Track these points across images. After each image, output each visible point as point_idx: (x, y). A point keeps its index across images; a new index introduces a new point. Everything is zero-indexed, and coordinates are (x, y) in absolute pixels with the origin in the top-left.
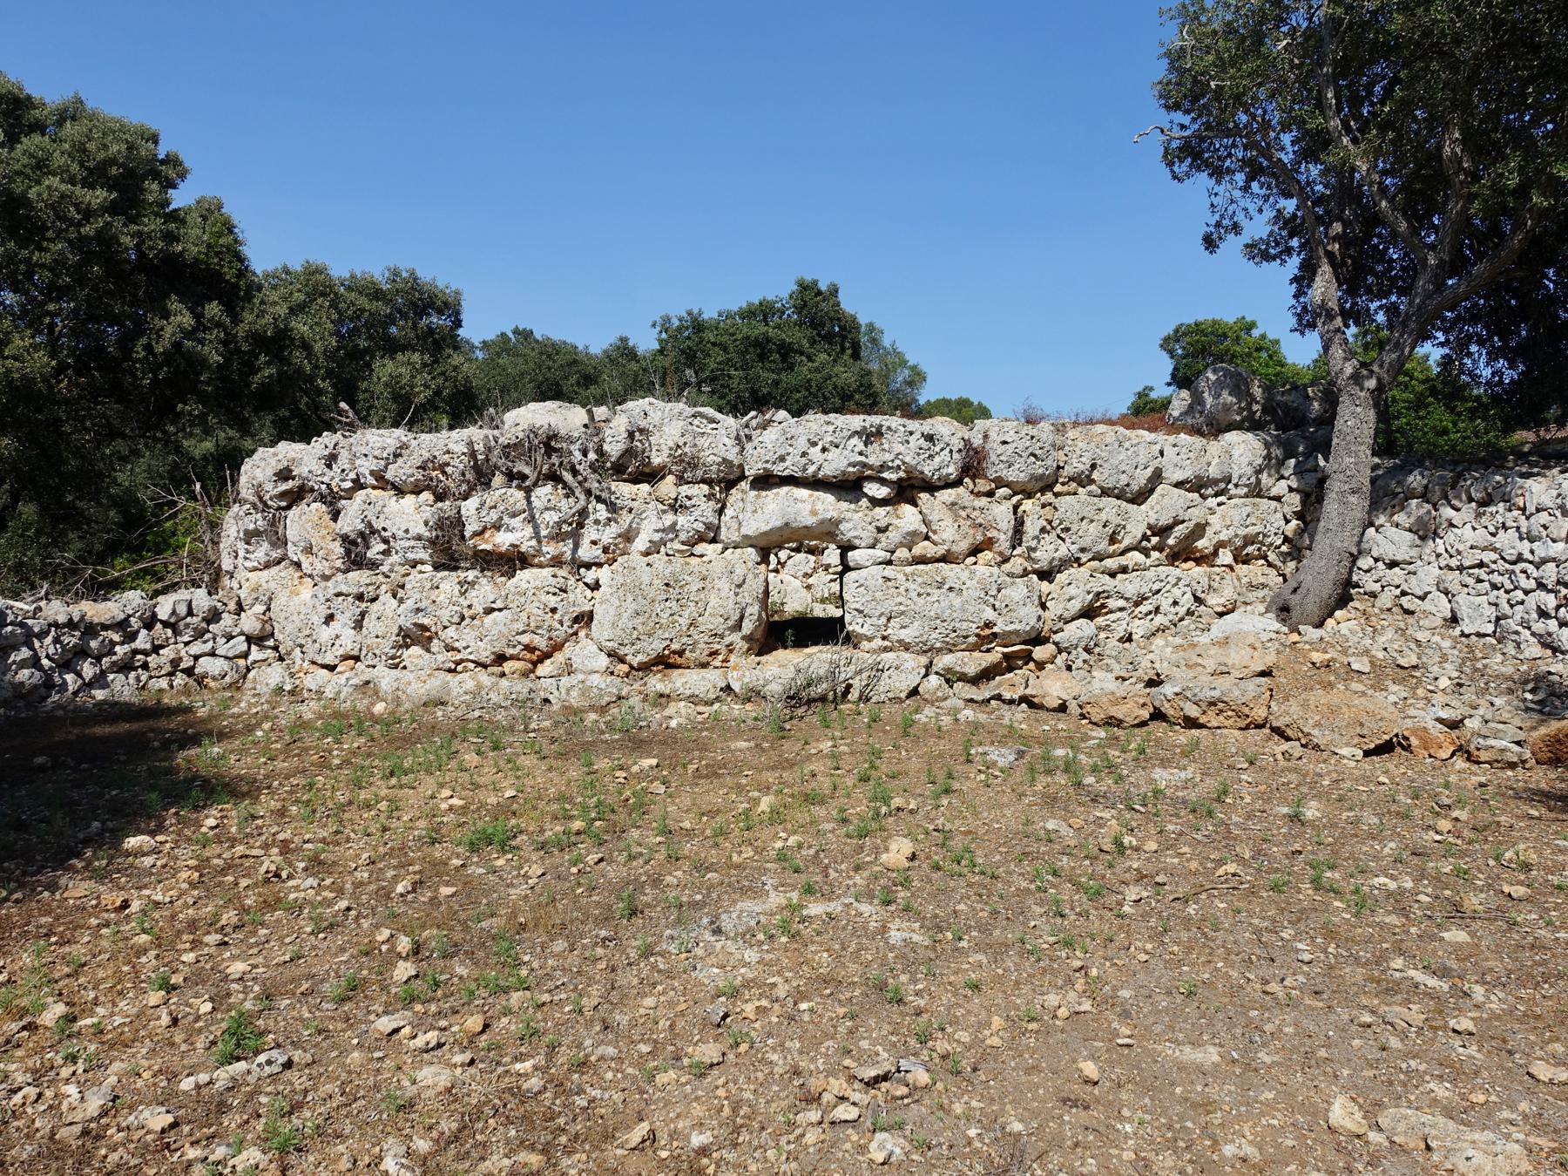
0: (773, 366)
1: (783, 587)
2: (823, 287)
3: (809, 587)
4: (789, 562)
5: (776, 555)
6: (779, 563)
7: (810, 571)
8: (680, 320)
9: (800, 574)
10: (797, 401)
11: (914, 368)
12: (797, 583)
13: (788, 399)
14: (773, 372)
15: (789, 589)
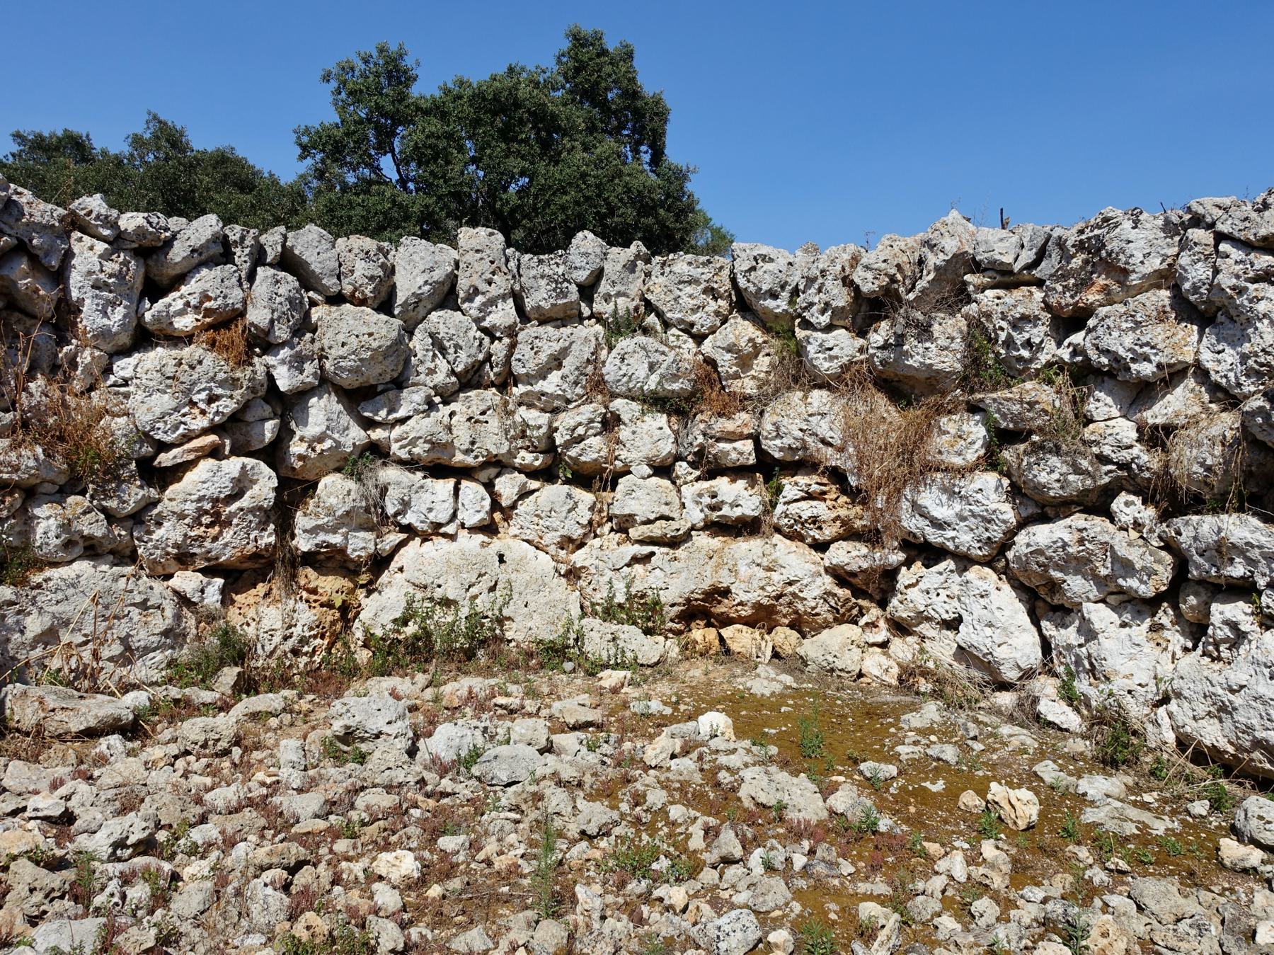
0: (524, 149)
1: (503, 574)
2: (611, 45)
3: (573, 574)
4: (523, 507)
5: (489, 486)
6: (495, 505)
7: (577, 533)
8: (366, 62)
9: (551, 538)
10: (563, 208)
11: (718, 230)
12: (544, 562)
13: (547, 203)
14: (523, 158)
15: (519, 580)
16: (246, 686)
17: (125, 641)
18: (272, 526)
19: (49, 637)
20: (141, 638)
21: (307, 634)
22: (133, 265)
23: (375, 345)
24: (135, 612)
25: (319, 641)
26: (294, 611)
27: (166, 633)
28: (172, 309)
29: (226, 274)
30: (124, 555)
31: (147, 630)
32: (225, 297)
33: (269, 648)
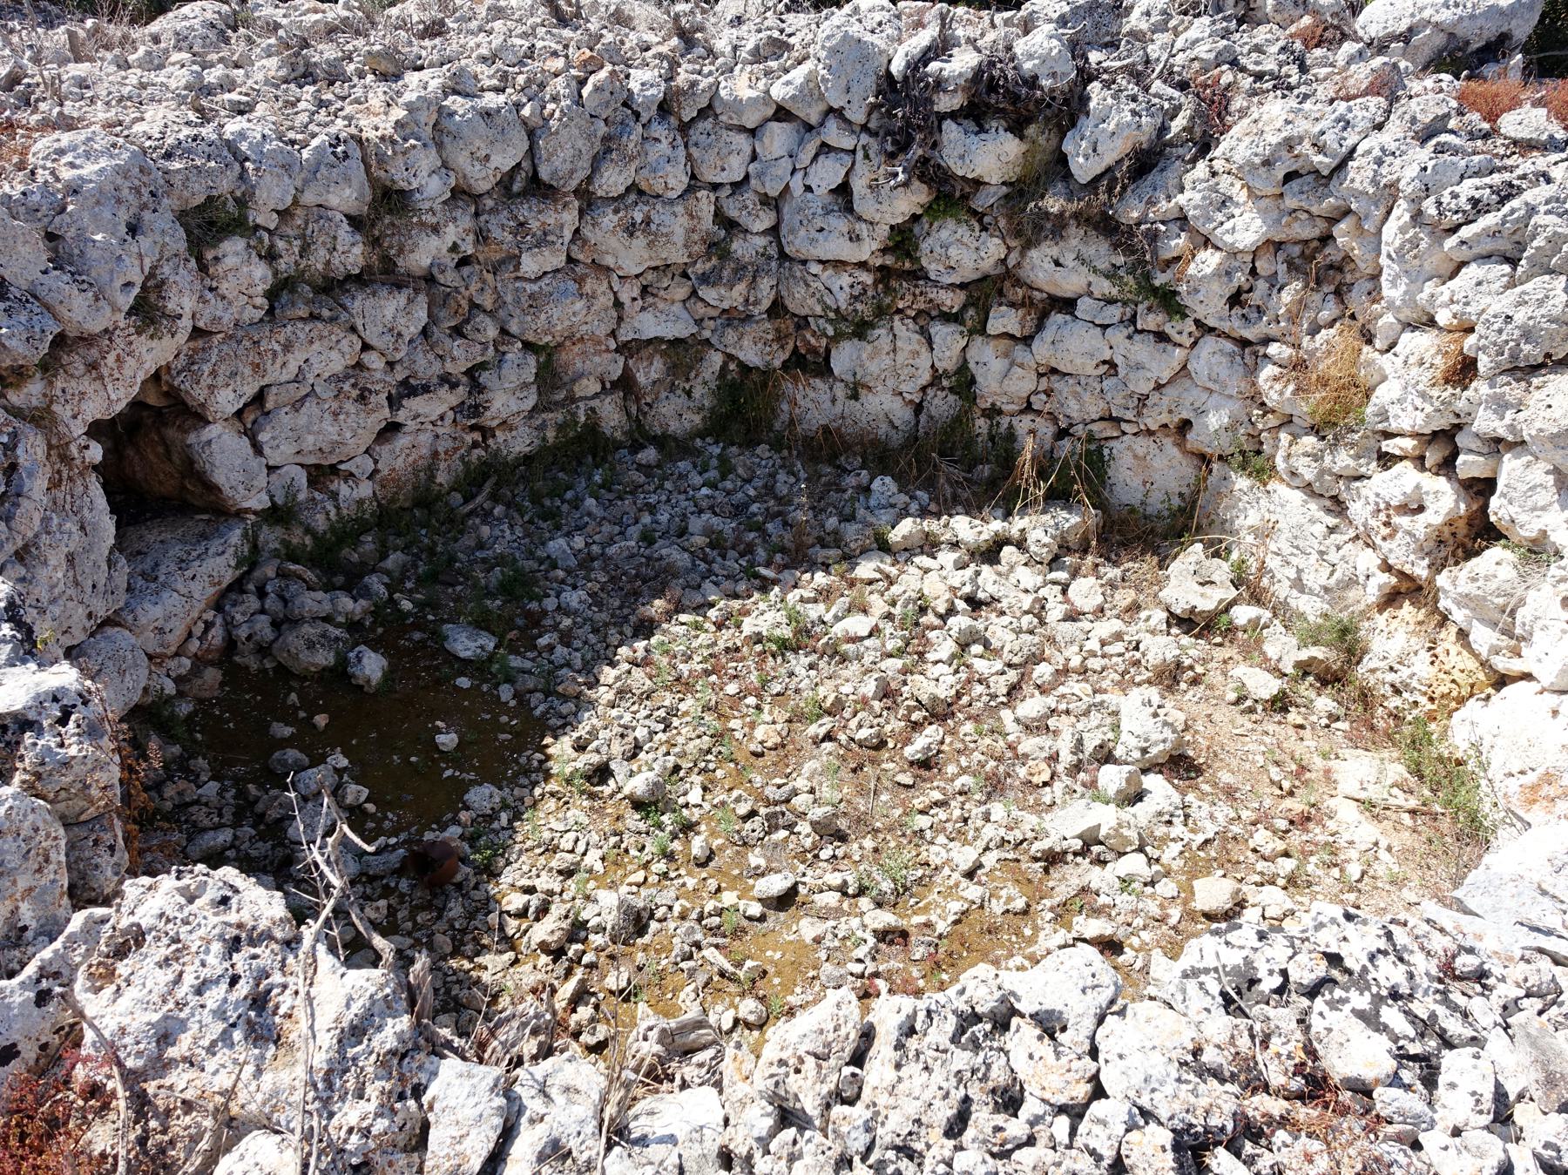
16: (1329, 679)
17: (1299, 571)
18: (1427, 561)
19: (1259, 533)
20: (1309, 579)
21: (1414, 684)
22: (1423, 245)
23: (1538, 425)
24: (1315, 556)
25: (1423, 700)
26: (1416, 653)
27: (1326, 589)
28: (1441, 299)
29: (1491, 276)
30: (1337, 506)
31: (1316, 577)
32: (1467, 304)
33: (1372, 665)
